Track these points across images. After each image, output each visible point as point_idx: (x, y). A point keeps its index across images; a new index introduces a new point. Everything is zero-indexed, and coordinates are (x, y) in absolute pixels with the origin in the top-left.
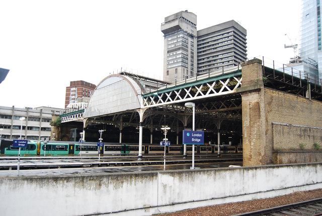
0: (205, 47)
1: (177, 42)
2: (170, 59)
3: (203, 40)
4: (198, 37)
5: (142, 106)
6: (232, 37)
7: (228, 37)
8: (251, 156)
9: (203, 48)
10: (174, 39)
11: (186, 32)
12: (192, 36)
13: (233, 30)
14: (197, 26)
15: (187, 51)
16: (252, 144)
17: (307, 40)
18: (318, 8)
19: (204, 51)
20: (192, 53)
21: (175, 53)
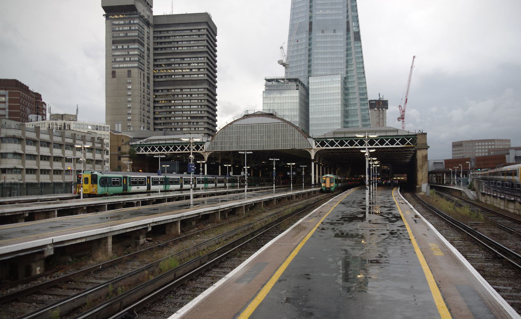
0: (165, 43)
1: (130, 30)
2: (117, 53)
3: (160, 32)
4: (156, 26)
5: (314, 147)
6: (205, 37)
7: (199, 35)
8: (422, 179)
10: (124, 25)
11: (142, 17)
13: (206, 27)
14: (154, 9)
15: (143, 45)
16: (423, 173)
18: (311, 24)
20: (148, 49)
21: (125, 47)
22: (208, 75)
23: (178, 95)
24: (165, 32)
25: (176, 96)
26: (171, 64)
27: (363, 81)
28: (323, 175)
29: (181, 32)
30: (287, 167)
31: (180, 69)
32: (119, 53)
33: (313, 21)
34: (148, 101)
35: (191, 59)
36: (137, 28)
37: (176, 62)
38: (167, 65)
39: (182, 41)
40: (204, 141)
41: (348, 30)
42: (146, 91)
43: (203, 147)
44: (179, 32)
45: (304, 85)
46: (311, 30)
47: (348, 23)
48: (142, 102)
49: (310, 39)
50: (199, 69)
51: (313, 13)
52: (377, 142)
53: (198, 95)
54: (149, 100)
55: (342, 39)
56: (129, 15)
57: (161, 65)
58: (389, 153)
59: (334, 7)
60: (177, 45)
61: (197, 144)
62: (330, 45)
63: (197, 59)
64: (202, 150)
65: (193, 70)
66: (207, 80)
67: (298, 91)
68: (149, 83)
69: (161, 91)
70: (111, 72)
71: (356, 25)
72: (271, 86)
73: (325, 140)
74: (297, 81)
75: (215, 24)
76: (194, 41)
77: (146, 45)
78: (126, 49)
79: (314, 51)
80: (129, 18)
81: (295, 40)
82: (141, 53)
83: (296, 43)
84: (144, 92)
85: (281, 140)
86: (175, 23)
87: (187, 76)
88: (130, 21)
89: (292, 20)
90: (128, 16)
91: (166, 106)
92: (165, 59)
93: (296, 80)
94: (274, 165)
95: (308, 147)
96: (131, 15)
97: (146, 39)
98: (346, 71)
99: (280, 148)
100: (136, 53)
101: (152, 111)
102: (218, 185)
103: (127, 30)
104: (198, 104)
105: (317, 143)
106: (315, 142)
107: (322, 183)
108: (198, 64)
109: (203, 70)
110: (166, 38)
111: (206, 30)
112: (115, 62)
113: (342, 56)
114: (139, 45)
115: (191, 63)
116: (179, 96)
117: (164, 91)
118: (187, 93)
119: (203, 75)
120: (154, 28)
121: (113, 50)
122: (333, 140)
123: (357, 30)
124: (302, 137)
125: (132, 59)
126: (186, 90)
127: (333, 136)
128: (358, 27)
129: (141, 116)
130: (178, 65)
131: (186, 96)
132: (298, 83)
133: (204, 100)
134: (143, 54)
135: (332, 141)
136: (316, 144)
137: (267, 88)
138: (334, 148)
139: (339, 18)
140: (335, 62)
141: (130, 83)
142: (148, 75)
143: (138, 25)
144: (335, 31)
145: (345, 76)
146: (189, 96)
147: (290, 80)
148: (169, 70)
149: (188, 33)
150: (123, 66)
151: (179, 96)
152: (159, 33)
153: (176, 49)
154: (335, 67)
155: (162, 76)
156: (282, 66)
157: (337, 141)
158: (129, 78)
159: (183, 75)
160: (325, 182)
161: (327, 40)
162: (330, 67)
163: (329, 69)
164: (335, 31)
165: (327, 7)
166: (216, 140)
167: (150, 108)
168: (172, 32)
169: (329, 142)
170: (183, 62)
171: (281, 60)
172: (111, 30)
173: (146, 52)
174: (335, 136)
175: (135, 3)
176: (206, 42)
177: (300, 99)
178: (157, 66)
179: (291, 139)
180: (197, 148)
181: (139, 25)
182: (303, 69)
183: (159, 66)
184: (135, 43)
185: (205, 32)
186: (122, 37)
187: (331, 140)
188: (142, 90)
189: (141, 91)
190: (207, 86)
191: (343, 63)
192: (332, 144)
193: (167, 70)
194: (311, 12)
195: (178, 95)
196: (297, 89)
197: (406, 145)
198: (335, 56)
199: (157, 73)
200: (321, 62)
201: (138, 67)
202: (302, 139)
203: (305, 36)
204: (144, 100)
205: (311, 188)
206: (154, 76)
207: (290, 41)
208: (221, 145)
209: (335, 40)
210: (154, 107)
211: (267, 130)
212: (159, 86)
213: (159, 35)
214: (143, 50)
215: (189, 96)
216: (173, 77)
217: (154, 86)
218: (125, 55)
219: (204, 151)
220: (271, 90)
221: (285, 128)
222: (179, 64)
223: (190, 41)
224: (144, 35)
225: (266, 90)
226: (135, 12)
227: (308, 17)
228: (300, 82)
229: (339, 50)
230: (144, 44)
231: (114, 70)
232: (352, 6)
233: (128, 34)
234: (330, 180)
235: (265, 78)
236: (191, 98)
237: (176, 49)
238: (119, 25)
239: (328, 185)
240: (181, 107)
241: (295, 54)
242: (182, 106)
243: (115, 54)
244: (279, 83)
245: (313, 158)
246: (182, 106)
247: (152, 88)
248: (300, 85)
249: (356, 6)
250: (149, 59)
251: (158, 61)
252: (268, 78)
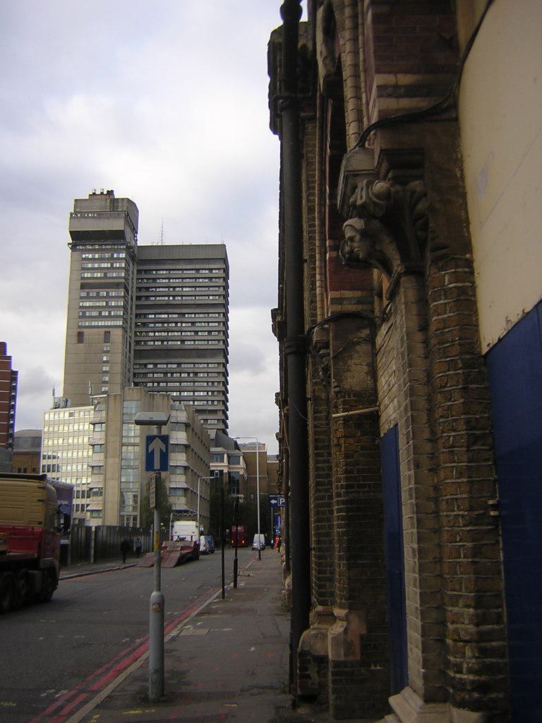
7: (211, 278)
10: (101, 260)
23: (172, 374)
32: (91, 304)
37: (171, 320)
50: (210, 332)
70: (76, 334)
78: (103, 297)
87: (189, 343)
88: (113, 255)
90: (110, 247)
103: (107, 268)
104: (209, 389)
112: (83, 317)
116: (175, 375)
121: (81, 298)
125: (112, 314)
131: (186, 375)
133: (219, 382)
141: (107, 352)
146: (191, 375)
150: (96, 324)
158: (107, 344)
170: (184, 320)
172: (78, 267)
186: (97, 278)
218: (103, 307)
231: (82, 330)
233: (108, 275)
236: (196, 379)
238: (93, 260)
242: (180, 392)
243: (85, 304)
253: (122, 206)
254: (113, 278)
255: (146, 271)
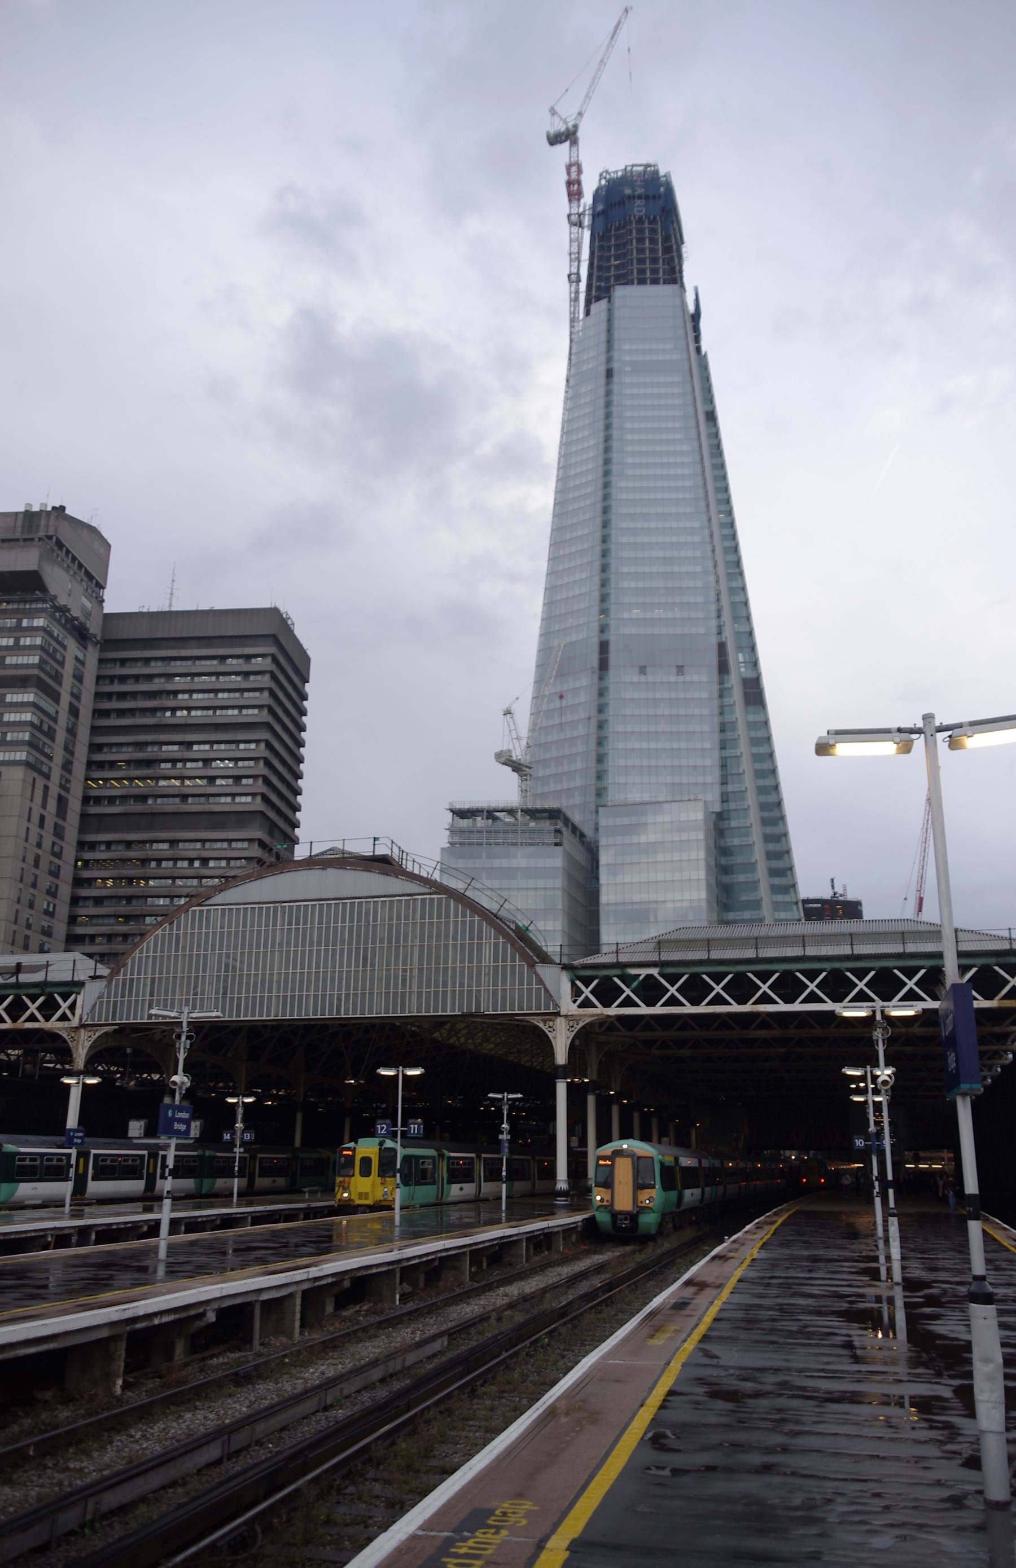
3: (123, 662)
4: (108, 644)
5: (568, 1006)
6: (265, 681)
7: (246, 674)
9: (122, 696)
11: (64, 610)
12: (82, 635)
13: (273, 650)
14: (107, 594)
15: (56, 697)
17: (554, 753)
18: (604, 647)
19: (122, 713)
20: (74, 712)
22: (265, 798)
23: (159, 861)
24: (139, 664)
25: (153, 864)
26: (149, 763)
27: (775, 814)
28: (603, 1139)
29: (189, 663)
30: (487, 1110)
31: (175, 778)
33: (612, 638)
34: (52, 879)
35: (215, 747)
36: (38, 641)
37: (164, 756)
38: (132, 765)
39: (191, 692)
40: (80, 976)
41: (723, 668)
42: (47, 843)
43: (74, 1002)
44: (184, 663)
45: (582, 835)
46: (604, 665)
47: (722, 647)
48: (29, 879)
49: (602, 693)
50: (238, 779)
51: (612, 616)
52: (861, 985)
53: (228, 863)
54: (55, 873)
55: (705, 695)
56: (19, 602)
57: (112, 765)
58: (908, 1049)
59: (677, 599)
60: (170, 703)
61: (48, 990)
62: (667, 712)
63: (233, 746)
64: (68, 1020)
65: (219, 782)
66: (262, 812)
67: (559, 848)
68: (64, 819)
69: (103, 847)
71: (747, 660)
72: (471, 832)
73: (618, 972)
74: (559, 818)
75: (305, 647)
76: (229, 691)
77: (66, 699)
79: (615, 727)
80: (17, 611)
81: (555, 693)
82: (45, 719)
83: (557, 703)
84: (39, 845)
85: (416, 973)
86: (172, 636)
88: (20, 621)
89: (547, 634)
90: (15, 606)
91: (119, 898)
92: (128, 744)
93: (554, 814)
94: (182, 1056)
95: (538, 1008)
96: (25, 602)
97: (68, 680)
98: (721, 741)
99: (413, 1009)
100: (27, 717)
101: (63, 910)
102: (95, 1187)
105: (583, 988)
106: (573, 984)
107: (595, 1190)
108: (236, 764)
109: (250, 781)
110: (141, 679)
111: (269, 660)
113: (707, 745)
114: (39, 693)
115: (215, 760)
117: (113, 847)
118: (192, 854)
119: (249, 799)
120: (101, 650)
122: (654, 971)
123: (753, 675)
124: (513, 960)
126: (187, 845)
127: (654, 957)
128: (755, 664)
129: (15, 927)
130: (169, 765)
131: (186, 864)
132: (560, 825)
134: (52, 724)
135: (649, 977)
136: (577, 993)
137: (456, 839)
138: (658, 1010)
139: (693, 631)
140: (684, 762)
142: (63, 793)
143: (42, 633)
144: (680, 669)
145: (717, 808)
146: (197, 864)
147: (532, 813)
148: (137, 778)
149: (213, 665)
151: (164, 864)
152: (118, 664)
153: (168, 714)
154: (684, 780)
155: (111, 800)
156: (510, 769)
157: (672, 980)
159: (184, 797)
160: (607, 1184)
161: (658, 695)
162: (669, 780)
163: (666, 784)
164: (680, 669)
165: (655, 600)
166: (132, 974)
167: (57, 902)
168: (159, 664)
169: (635, 984)
171: (505, 748)
173: (63, 718)
174: (665, 957)
175: (39, 566)
176: (266, 694)
177: (570, 877)
178: (101, 765)
179: (462, 968)
180: (49, 1008)
181: (50, 634)
182: (578, 782)
183: (107, 766)
184: (25, 687)
185: (266, 664)
187: (644, 972)
188: (33, 839)
189: (26, 840)
190: (259, 834)
191: (711, 766)
192: (650, 991)
193: (131, 779)
194: (604, 611)
195: (159, 861)
196: (556, 844)
197: (1005, 998)
198: (683, 745)
199: (100, 787)
200: (637, 762)
201: (27, 764)
202: (513, 968)
203: (585, 680)
204: (37, 872)
205: (550, 1212)
206: (86, 800)
207: (537, 698)
208: (152, 995)
209: (681, 695)
210: (75, 900)
211: (359, 927)
212: (98, 831)
213: (119, 671)
214: (52, 711)
215: (197, 864)
216: (150, 801)
217: (83, 829)
219: (75, 1022)
220: (469, 844)
221: (439, 917)
222: (174, 761)
223: (216, 691)
224: (62, 664)
225: (452, 844)
226: (37, 592)
227: (595, 626)
228: (567, 821)
229: (698, 728)
230: (59, 694)
232: (733, 604)
234: (637, 1172)
235: (451, 804)
236: (205, 872)
237: (168, 714)
239: (624, 1202)
240: (167, 901)
241: (555, 736)
244: (498, 823)
245: (561, 1058)
246: (172, 897)
247: (72, 835)
248: (566, 833)
249: (746, 603)
250: (74, 743)
251: (105, 750)
252: (458, 806)
253: (47, 526)
254: (17, 666)
255: (114, 661)
